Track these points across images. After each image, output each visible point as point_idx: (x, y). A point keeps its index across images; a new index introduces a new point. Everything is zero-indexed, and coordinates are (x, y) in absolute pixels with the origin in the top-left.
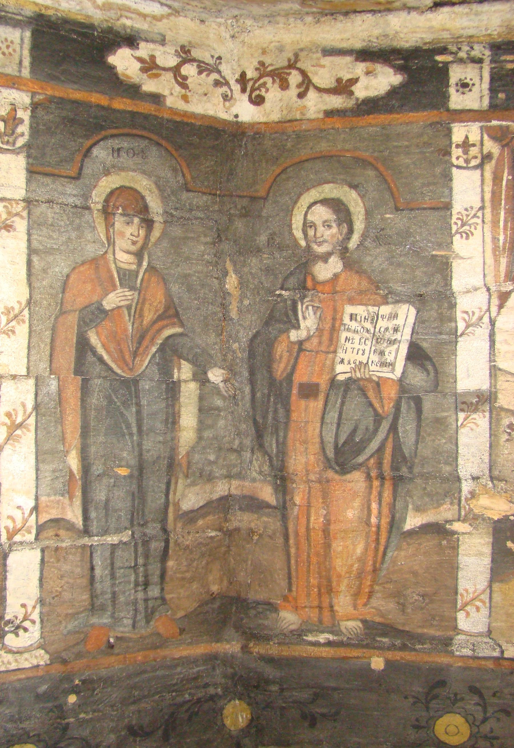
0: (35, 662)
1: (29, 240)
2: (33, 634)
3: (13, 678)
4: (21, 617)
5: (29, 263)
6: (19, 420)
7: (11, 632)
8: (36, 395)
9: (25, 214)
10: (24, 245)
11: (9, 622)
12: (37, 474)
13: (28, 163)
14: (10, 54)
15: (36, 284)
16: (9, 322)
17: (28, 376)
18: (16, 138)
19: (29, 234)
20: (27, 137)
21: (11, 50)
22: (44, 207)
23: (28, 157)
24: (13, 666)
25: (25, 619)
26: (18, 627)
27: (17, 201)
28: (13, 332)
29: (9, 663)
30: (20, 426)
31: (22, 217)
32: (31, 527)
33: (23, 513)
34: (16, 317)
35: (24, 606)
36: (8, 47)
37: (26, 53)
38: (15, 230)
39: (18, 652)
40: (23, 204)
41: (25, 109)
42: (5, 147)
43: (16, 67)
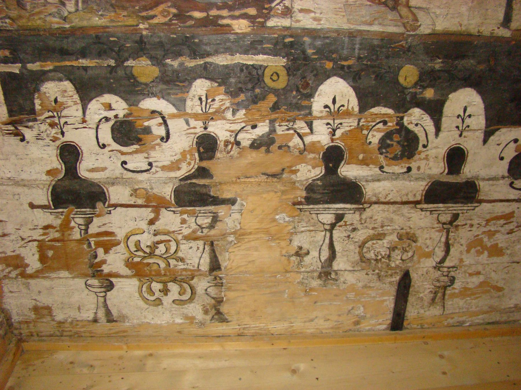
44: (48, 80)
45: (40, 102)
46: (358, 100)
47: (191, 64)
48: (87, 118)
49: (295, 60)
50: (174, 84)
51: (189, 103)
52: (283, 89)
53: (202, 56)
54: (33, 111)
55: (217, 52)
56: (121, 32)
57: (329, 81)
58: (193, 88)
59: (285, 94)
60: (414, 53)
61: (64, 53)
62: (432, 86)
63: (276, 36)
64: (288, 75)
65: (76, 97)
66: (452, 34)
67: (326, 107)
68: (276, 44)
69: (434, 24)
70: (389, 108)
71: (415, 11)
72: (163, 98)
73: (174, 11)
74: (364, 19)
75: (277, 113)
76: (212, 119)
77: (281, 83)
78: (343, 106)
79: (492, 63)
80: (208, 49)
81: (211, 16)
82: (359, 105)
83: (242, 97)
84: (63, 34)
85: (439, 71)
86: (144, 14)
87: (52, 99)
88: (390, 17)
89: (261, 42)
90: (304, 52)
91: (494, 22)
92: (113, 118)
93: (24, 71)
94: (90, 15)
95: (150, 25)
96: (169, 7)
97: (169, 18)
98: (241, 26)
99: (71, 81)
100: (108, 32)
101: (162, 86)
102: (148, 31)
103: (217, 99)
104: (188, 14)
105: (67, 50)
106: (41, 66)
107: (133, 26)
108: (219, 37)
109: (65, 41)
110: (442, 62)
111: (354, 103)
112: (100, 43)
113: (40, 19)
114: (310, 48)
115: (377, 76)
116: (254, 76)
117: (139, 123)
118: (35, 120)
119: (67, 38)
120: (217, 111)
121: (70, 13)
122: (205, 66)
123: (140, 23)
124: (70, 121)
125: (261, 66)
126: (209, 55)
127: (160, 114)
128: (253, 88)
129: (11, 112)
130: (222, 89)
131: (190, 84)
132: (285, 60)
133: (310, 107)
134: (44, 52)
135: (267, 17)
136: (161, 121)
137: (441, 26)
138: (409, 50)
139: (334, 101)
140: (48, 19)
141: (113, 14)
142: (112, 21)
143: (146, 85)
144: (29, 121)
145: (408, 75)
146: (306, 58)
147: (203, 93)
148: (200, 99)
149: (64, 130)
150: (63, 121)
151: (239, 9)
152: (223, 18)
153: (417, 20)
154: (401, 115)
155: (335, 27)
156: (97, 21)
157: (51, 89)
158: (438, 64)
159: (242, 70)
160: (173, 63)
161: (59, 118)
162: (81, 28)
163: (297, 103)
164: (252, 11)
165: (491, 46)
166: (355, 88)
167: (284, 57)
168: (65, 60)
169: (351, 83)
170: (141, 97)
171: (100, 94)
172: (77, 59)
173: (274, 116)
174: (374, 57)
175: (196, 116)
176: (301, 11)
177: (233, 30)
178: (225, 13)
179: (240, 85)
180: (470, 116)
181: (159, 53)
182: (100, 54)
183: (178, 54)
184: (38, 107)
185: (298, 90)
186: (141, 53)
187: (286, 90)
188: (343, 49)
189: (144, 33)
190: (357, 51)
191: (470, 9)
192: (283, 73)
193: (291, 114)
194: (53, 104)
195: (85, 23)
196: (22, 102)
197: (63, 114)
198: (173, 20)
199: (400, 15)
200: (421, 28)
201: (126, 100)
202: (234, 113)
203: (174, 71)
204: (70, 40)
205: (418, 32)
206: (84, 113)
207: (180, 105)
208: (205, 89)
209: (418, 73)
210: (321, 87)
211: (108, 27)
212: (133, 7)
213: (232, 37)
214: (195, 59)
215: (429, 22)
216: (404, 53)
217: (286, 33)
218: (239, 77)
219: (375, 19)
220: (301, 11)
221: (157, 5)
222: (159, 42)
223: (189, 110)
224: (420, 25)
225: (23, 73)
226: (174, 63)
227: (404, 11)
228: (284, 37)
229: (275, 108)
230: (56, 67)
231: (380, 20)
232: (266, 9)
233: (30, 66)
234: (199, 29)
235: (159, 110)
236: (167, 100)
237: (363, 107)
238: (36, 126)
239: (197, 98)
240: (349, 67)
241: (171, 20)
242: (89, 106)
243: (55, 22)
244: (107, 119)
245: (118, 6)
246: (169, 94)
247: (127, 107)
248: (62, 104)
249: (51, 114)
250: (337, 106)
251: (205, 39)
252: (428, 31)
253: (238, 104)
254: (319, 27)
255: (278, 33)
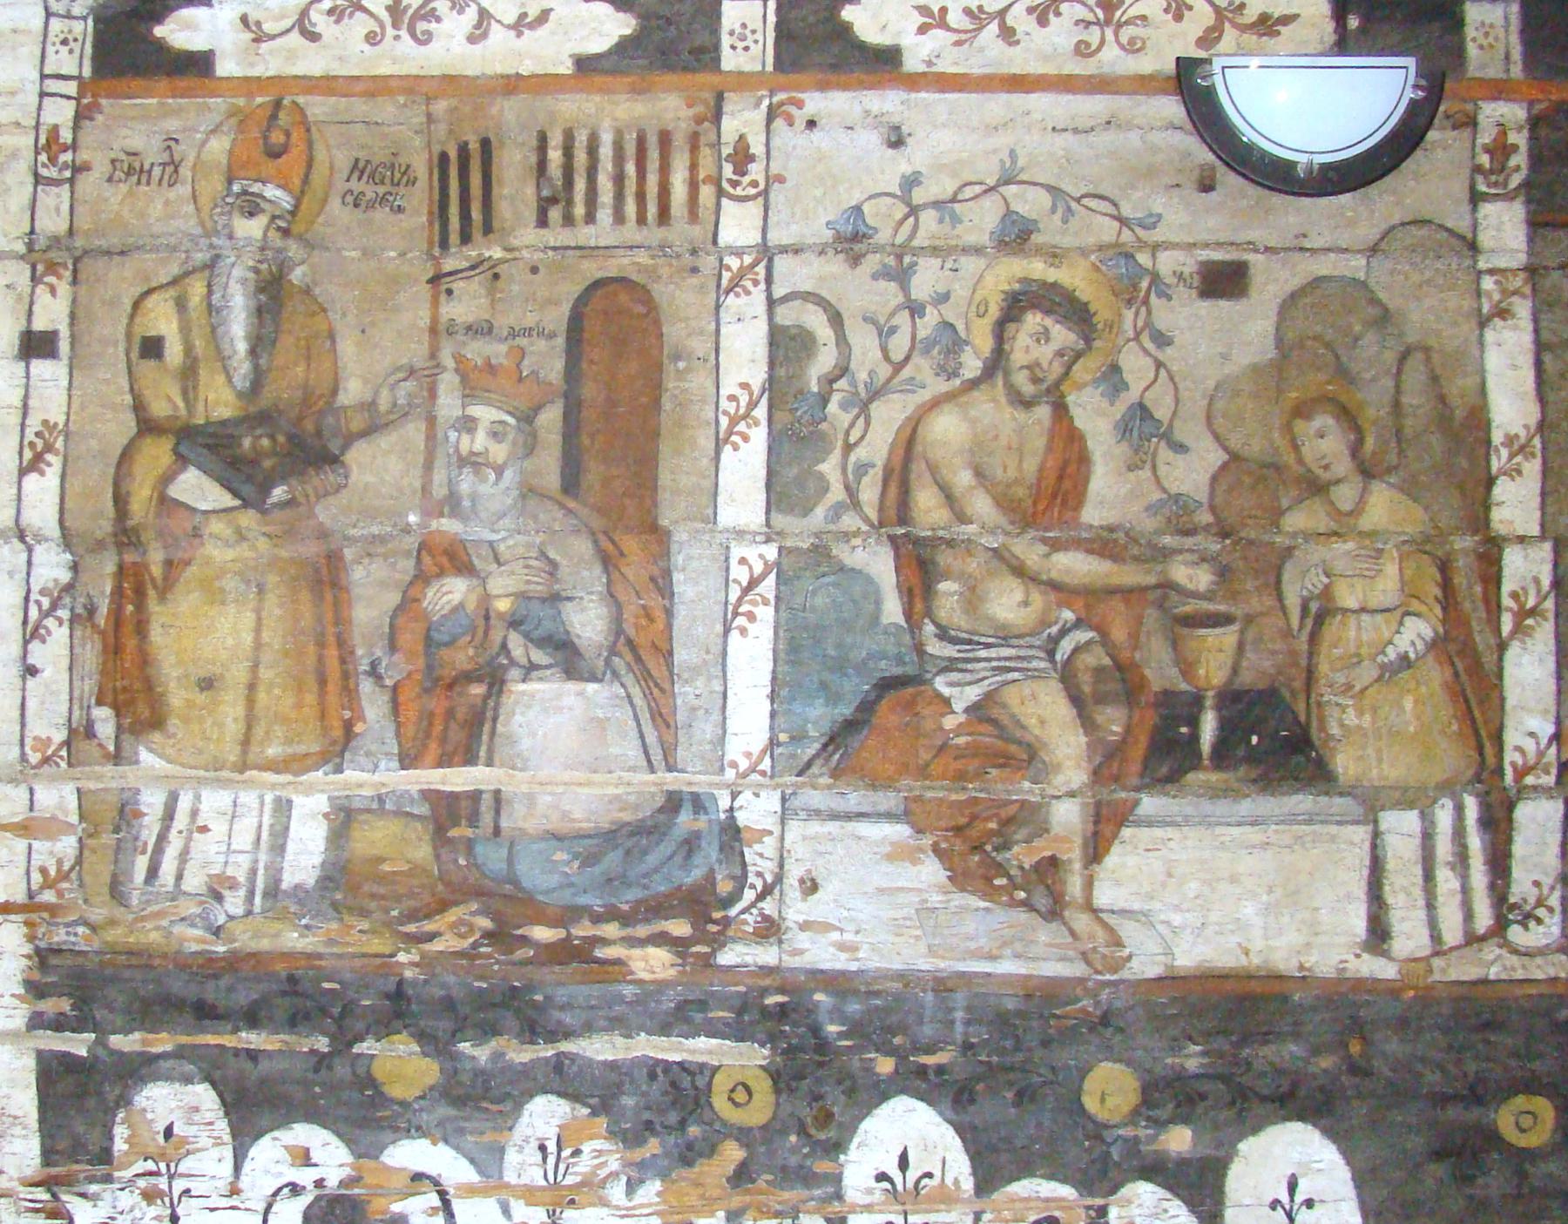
0: (1552, 972)
1: (1536, 331)
2: (1548, 931)
3: (1519, 992)
4: (1532, 901)
5: (1538, 365)
6: (1531, 603)
7: (1517, 922)
8: (1556, 565)
9: (1527, 290)
10: (1527, 338)
11: (1514, 907)
12: (1558, 685)
13: (1528, 212)
14: (1491, 46)
15: (1551, 397)
16: (1511, 457)
17: (1543, 537)
18: (1509, 176)
19: (1536, 320)
20: (1524, 172)
21: (1491, 39)
22: (1556, 274)
23: (1528, 202)
24: (1519, 974)
25: (1540, 902)
26: (1528, 916)
27: (1514, 271)
28: (1519, 472)
29: (1513, 969)
30: (1533, 612)
31: (1523, 296)
32: (1549, 763)
33: (1538, 743)
34: (1522, 449)
35: (1536, 884)
36: (1487, 34)
37: (1514, 39)
38: (1513, 316)
39: (1525, 955)
40: (1522, 275)
41: (1520, 129)
42: (1493, 191)
43: (1500, 66)
44: (156, 1078)
45: (127, 1133)
46: (972, 1159)
47: (522, 1055)
48: (244, 1183)
49: (790, 1052)
50: (475, 1104)
51: (511, 1157)
52: (764, 1128)
53: (553, 1036)
54: (105, 1156)
55: (588, 1029)
56: (352, 970)
57: (886, 1109)
58: (525, 1119)
59: (767, 1141)
60: (1121, 1030)
61: (205, 1013)
62: (1185, 1121)
63: (742, 989)
64: (777, 1091)
65: (222, 1126)
66: (1223, 976)
67: (882, 1177)
68: (740, 1012)
69: (1168, 952)
70: (1064, 1181)
71: (1112, 920)
72: (446, 1141)
73: (485, 923)
74: (973, 945)
75: (748, 1192)
76: (572, 1202)
77: (759, 1112)
78: (929, 1175)
79: (1355, 1048)
80: (567, 1019)
81: (577, 938)
82: (974, 1173)
83: (653, 1146)
84: (210, 968)
85: (1197, 1076)
86: (411, 928)
87: (161, 1127)
88: (1043, 938)
89: (702, 1005)
90: (816, 1031)
91: (1343, 940)
92: (310, 1187)
93: (101, 1052)
94: (277, 926)
95: (423, 955)
96: (473, 914)
97: (471, 940)
98: (652, 963)
99: (214, 1085)
100: (319, 968)
101: (444, 1111)
102: (417, 970)
103: (587, 1147)
104: (519, 932)
105: (214, 1007)
106: (144, 1042)
107: (383, 956)
108: (596, 990)
109: (211, 985)
110: (1204, 1053)
111: (960, 1168)
112: (296, 993)
113: (157, 928)
114: (832, 1022)
115: (1020, 1094)
116: (684, 1091)
117: (377, 1203)
118: (108, 1179)
119: (216, 977)
120: (586, 1183)
121: (231, 918)
122: (559, 1064)
123: (399, 950)
124: (197, 1187)
125: (702, 1066)
126: (567, 1035)
127: (436, 1182)
128: (683, 1124)
129: (48, 1155)
130: (602, 1122)
131: (518, 1107)
132: (766, 1052)
133: (838, 1179)
134: (153, 1009)
135: (718, 942)
136: (435, 1200)
137: (1189, 956)
138: (1105, 1020)
139: (903, 1163)
140: (178, 929)
141: (334, 926)
142: (331, 942)
143: (403, 1104)
144: (92, 1180)
145: (1109, 1089)
146: (822, 1045)
147: (551, 1133)
148: (543, 1148)
149: (180, 1211)
150: (179, 1185)
151: (647, 920)
152: (604, 942)
153: (1119, 943)
154: (1099, 1201)
155: (897, 965)
156: (293, 940)
157: (160, 1101)
158: (1192, 1059)
159: (652, 1076)
160: (476, 1052)
161: (171, 1177)
162: (253, 955)
163: (801, 1167)
164: (680, 928)
165: (1346, 1008)
166: (960, 1130)
167: (762, 1045)
168: (203, 1031)
169: (949, 1113)
170: (388, 1135)
171: (285, 1122)
172: (236, 1030)
173: (737, 1201)
174: (1008, 1043)
175: (530, 1194)
176: (805, 926)
177: (632, 973)
178: (611, 930)
179: (647, 1116)
180: (1309, 1203)
181: (443, 1026)
182: (294, 1022)
183: (489, 1031)
184: (120, 1146)
185: (802, 1131)
186: (397, 1024)
187: (771, 1131)
188: (921, 1023)
189: (408, 974)
190: (959, 1028)
191: (1267, 909)
192: (762, 1087)
193: (786, 1195)
194: (161, 1139)
195: (265, 944)
196: (81, 1129)
197: (182, 1168)
198: (483, 945)
199: (1073, 933)
200: (1134, 963)
201: (349, 1142)
202: (631, 1188)
203: (479, 1073)
204: (224, 982)
205: (1125, 974)
206: (237, 1168)
207: (488, 1160)
208: (556, 1121)
209: (1137, 1085)
210: (866, 1125)
211: (320, 956)
212: (387, 912)
213: (628, 991)
214: (532, 1042)
215: (1153, 946)
216: (1091, 1029)
217: (767, 982)
218: (644, 1094)
219: (1005, 944)
220: (805, 926)
221: (443, 906)
222: (442, 999)
223: (510, 1177)
224: (1130, 957)
225: (96, 1058)
226: (475, 1052)
227: (1081, 922)
228: (765, 992)
229: (742, 1176)
230: (182, 1047)
231: (1018, 947)
232: (715, 922)
233: (117, 1041)
234: (545, 970)
235: (434, 1174)
236: (457, 1148)
237: (987, 1179)
238: (107, 1196)
239: (534, 1144)
240: (940, 1070)
241: (475, 945)
242: (252, 1152)
243: (193, 939)
244: (295, 1189)
245: (350, 909)
246: (461, 1131)
247: (349, 1159)
248: (184, 1141)
249: (150, 1166)
250: (912, 1175)
251: (561, 995)
252: (1153, 971)
253: (641, 1165)
254: (854, 967)
255: (749, 981)
